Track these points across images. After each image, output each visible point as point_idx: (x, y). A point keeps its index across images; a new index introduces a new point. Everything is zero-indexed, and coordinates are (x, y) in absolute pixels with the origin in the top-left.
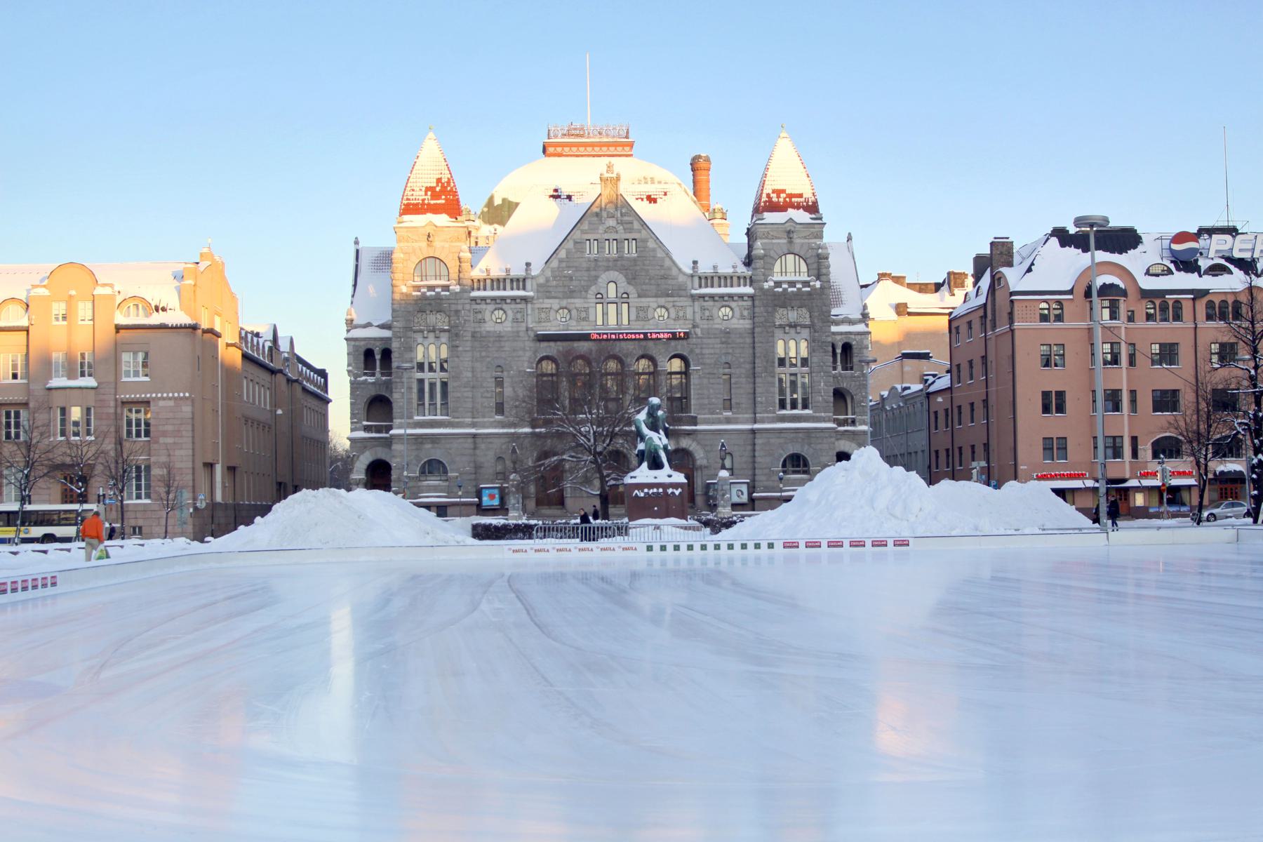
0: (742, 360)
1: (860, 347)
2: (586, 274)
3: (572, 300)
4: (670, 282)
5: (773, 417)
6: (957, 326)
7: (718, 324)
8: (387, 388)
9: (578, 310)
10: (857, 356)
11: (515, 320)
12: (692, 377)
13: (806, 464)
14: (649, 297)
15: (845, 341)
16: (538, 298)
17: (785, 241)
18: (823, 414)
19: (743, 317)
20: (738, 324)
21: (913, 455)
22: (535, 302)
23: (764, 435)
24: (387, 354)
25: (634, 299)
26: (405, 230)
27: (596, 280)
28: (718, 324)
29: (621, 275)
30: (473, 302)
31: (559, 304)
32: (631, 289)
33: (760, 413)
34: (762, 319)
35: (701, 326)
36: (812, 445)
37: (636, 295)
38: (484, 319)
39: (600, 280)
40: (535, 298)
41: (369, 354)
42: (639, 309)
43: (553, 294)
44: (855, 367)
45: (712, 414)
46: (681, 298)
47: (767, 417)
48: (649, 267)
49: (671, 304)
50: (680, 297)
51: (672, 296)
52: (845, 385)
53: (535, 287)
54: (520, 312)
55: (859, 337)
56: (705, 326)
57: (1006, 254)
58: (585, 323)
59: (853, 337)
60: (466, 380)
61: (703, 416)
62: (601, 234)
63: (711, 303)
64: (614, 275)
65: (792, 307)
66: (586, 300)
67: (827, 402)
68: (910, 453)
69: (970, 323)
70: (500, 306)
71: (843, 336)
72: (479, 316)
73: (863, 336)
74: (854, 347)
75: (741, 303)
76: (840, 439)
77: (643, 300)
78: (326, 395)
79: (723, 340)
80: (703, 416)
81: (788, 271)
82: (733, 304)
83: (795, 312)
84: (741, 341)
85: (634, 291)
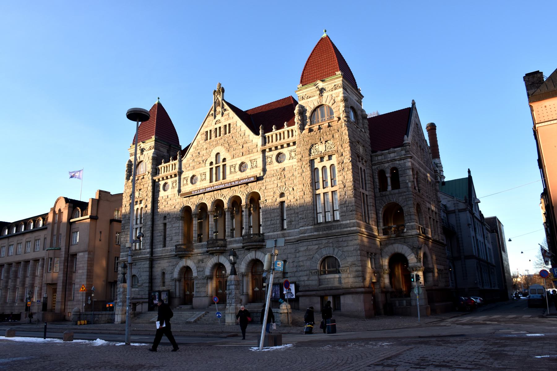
1: (403, 169)
2: (205, 151)
4: (248, 145)
5: (311, 228)
7: (276, 166)
10: (402, 177)
11: (173, 187)
15: (392, 166)
17: (317, 97)
18: (348, 221)
19: (291, 158)
20: (289, 163)
23: (305, 244)
25: (228, 163)
28: (276, 166)
31: (192, 173)
32: (228, 156)
33: (302, 227)
36: (340, 248)
37: (230, 158)
44: (401, 186)
45: (274, 231)
47: (308, 229)
49: (248, 159)
55: (402, 161)
57: (537, 83)
58: (204, 182)
59: (397, 162)
60: (148, 226)
61: (268, 234)
62: (213, 126)
63: (271, 153)
64: (219, 149)
65: (321, 142)
67: (351, 211)
71: (390, 163)
73: (405, 161)
74: (399, 170)
75: (290, 148)
76: (394, 243)
80: (268, 234)
83: (324, 145)
85: (229, 156)
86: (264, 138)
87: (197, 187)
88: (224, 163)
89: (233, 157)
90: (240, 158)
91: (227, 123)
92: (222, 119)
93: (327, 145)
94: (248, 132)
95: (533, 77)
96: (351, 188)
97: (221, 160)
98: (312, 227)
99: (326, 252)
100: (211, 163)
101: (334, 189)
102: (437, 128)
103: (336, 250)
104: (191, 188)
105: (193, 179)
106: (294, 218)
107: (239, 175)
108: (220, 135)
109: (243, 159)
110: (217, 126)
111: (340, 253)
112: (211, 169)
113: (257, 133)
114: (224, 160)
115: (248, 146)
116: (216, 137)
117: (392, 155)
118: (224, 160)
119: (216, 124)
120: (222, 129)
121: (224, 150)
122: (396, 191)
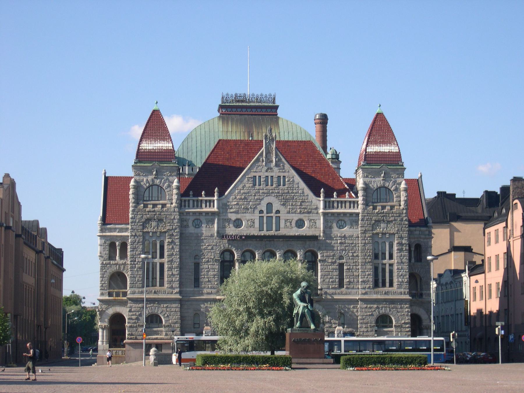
0: (350, 254)
2: (253, 197)
3: (244, 214)
6: (488, 232)
7: (337, 231)
8: (124, 268)
9: (248, 221)
12: (319, 264)
13: (391, 322)
14: (292, 213)
16: (223, 213)
21: (459, 315)
22: (221, 215)
24: (124, 246)
25: (283, 216)
26: (139, 168)
27: (260, 201)
29: (276, 199)
30: (182, 214)
34: (364, 229)
35: (326, 232)
37: (286, 212)
38: (188, 225)
39: (262, 202)
40: (221, 212)
41: (112, 246)
42: (286, 220)
43: (232, 210)
44: (423, 261)
46: (314, 214)
48: (293, 195)
50: (313, 213)
51: (309, 213)
52: (416, 271)
53: (221, 205)
54: (211, 221)
55: (426, 240)
56: (328, 233)
58: (252, 229)
59: (422, 240)
62: (263, 173)
63: (332, 218)
64: (271, 199)
65: (384, 221)
66: (253, 214)
68: (458, 314)
69: (497, 231)
70: (198, 217)
71: (416, 240)
72: (185, 223)
73: (428, 240)
77: (289, 215)
78: (60, 266)
79: (339, 241)
81: (381, 198)
82: (346, 219)
84: (351, 242)
86: (325, 202)
87: (242, 232)
88: (278, 215)
89: (289, 212)
90: (297, 215)
91: (282, 175)
92: (276, 169)
93: (389, 225)
94: (307, 191)
95: (519, 183)
96: (407, 264)
97: (274, 211)
98: (372, 290)
99: (382, 311)
100: (261, 212)
101: (391, 261)
102: (329, 121)
103: (392, 310)
104: (235, 232)
105: (238, 223)
106: (352, 279)
107: (295, 232)
108: (272, 185)
109: (302, 216)
110: (269, 174)
111: (395, 313)
112: (261, 218)
113: (318, 195)
114: (278, 212)
115: (307, 204)
116: (267, 185)
117: (417, 232)
118: (278, 212)
119: (266, 171)
120: (275, 180)
121: (277, 201)
122: (420, 264)
